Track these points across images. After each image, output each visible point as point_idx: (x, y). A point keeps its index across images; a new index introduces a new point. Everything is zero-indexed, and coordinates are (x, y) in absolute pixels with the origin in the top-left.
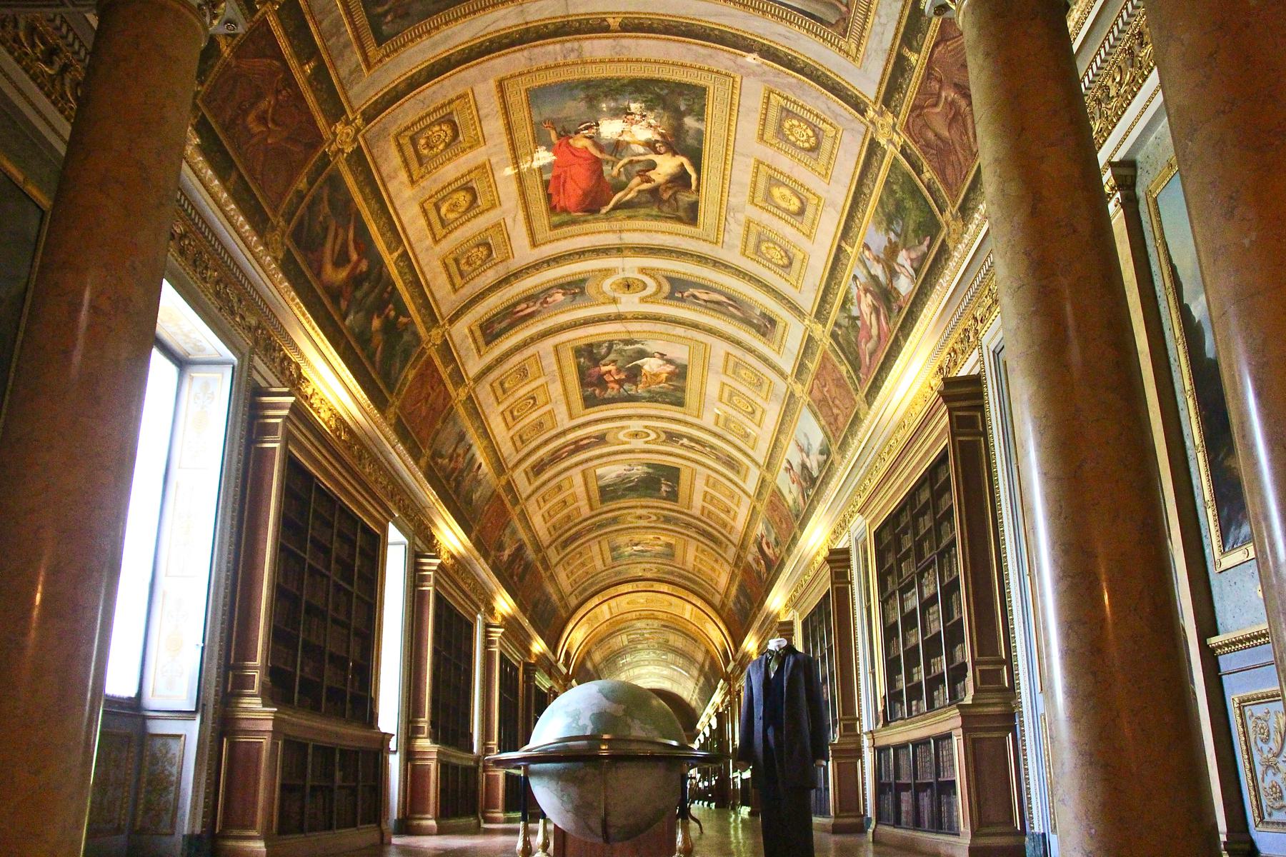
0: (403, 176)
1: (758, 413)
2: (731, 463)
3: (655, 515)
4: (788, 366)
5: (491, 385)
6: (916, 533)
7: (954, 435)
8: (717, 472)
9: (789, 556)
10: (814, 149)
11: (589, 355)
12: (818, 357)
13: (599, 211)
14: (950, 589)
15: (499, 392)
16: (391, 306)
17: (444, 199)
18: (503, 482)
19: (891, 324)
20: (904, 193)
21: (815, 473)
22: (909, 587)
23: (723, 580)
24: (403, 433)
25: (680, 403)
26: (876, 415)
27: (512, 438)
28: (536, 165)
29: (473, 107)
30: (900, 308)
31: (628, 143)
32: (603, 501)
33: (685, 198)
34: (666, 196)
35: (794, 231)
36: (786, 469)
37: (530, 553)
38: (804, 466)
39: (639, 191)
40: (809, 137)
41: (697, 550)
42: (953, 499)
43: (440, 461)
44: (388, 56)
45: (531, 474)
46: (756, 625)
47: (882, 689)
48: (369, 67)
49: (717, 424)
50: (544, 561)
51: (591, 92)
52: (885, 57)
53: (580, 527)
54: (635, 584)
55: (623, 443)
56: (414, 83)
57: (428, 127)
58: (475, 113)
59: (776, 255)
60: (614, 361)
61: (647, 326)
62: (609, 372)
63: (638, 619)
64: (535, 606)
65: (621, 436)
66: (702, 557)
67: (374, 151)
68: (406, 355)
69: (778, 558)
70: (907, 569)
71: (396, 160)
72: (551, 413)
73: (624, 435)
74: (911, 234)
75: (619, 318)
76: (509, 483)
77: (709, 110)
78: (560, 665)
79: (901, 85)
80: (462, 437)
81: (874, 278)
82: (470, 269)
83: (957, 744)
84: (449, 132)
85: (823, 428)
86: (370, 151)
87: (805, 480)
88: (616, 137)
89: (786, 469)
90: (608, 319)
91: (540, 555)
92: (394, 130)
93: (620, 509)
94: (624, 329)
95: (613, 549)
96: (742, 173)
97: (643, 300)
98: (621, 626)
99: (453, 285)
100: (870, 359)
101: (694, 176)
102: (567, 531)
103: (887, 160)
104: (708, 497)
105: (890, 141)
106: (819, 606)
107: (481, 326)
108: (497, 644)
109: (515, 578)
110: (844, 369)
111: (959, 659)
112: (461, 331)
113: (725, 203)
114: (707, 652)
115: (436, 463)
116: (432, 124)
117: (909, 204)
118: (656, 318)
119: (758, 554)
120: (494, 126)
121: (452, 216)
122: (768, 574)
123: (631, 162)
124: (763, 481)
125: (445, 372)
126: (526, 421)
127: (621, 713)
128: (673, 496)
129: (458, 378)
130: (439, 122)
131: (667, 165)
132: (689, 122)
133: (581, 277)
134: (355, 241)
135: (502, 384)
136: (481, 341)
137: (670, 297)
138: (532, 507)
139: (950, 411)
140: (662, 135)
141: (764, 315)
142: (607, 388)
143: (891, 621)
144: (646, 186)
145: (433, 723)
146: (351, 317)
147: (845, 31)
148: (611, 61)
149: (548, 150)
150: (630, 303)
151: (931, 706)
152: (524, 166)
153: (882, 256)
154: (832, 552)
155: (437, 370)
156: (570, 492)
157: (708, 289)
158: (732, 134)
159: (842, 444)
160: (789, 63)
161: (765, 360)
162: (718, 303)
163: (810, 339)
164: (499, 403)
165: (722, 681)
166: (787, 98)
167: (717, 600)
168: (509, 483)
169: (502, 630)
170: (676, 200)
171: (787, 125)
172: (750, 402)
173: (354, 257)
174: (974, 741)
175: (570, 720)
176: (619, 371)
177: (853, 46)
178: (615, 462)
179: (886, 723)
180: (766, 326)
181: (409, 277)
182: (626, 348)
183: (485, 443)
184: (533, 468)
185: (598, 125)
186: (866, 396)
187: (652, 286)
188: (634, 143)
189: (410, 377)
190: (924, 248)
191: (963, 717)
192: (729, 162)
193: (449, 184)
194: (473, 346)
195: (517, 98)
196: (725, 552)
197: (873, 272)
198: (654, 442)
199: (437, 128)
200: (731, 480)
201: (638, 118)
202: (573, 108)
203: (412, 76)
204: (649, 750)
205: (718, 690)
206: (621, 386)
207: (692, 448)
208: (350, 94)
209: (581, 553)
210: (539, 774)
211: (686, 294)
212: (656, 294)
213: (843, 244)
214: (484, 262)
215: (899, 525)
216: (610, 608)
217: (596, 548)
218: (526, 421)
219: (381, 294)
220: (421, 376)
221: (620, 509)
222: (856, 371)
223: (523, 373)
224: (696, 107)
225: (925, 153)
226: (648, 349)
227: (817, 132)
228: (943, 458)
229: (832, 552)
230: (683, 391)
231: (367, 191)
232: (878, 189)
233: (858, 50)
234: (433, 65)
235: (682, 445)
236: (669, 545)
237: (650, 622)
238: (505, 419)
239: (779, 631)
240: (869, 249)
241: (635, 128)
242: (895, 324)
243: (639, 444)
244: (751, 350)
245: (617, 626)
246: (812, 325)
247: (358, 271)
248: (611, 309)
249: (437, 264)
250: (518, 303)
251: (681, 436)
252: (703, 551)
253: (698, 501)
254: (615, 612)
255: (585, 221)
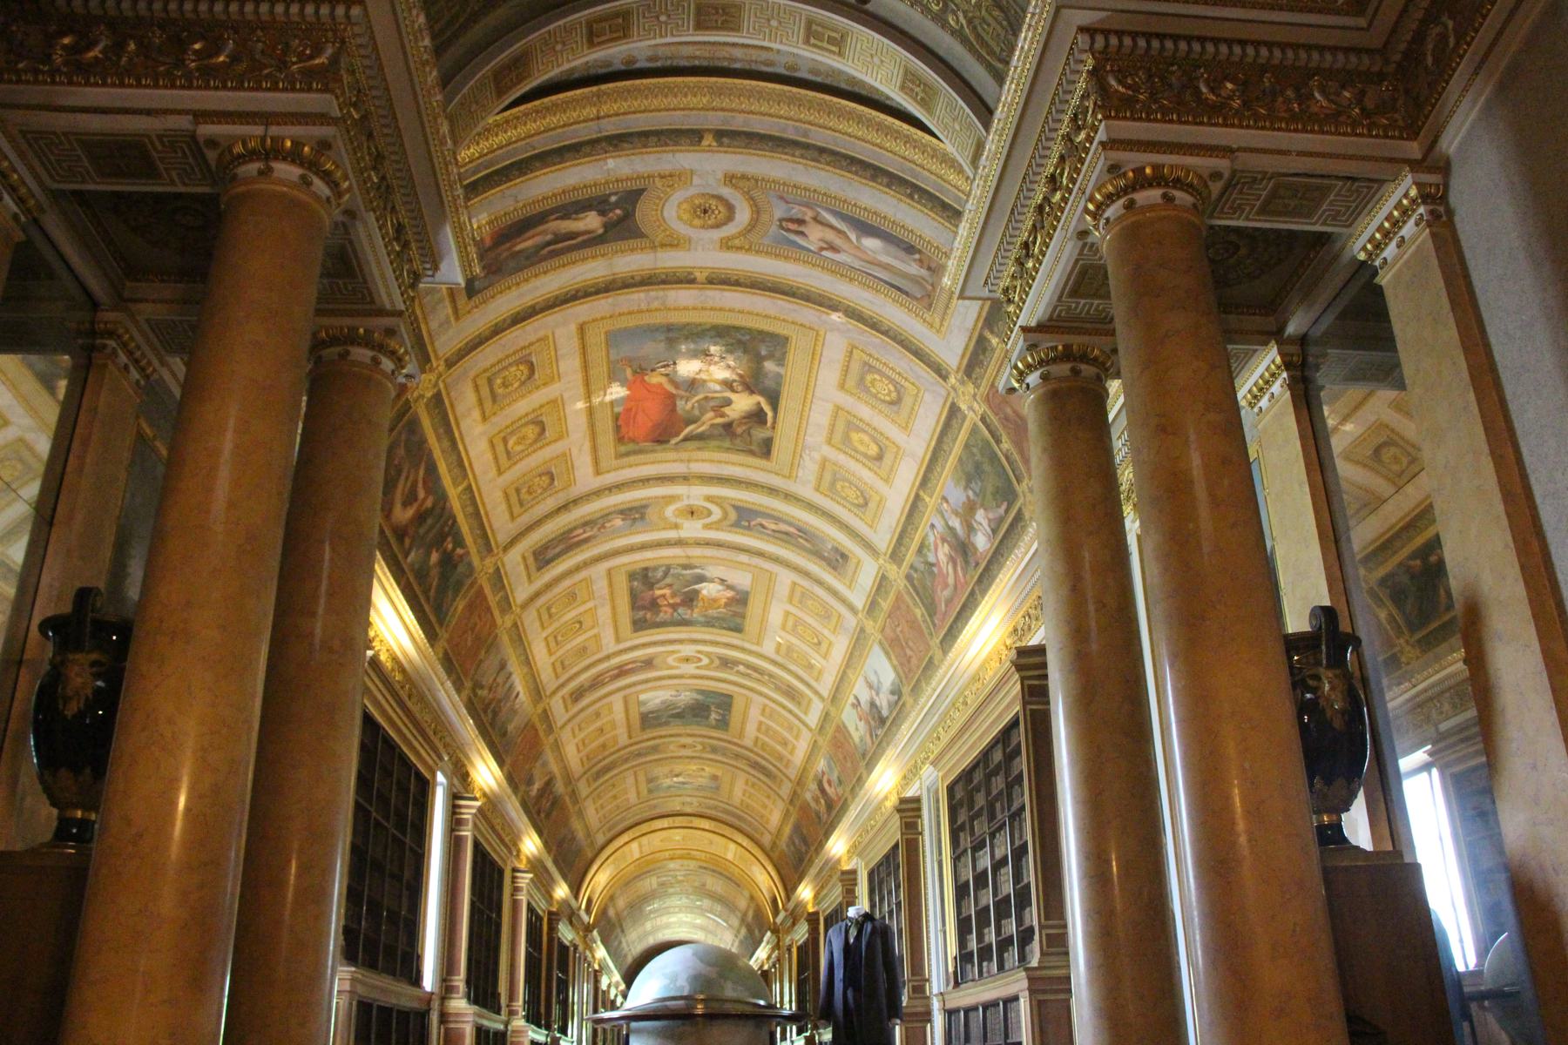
0: (476, 414)
1: (824, 646)
2: (791, 693)
3: (702, 744)
4: (859, 601)
5: (538, 611)
6: (988, 793)
7: (1025, 704)
8: (774, 701)
9: (854, 798)
10: (892, 403)
11: (644, 578)
12: (892, 596)
13: (667, 442)
14: (1020, 853)
15: (545, 617)
16: (449, 539)
17: (512, 433)
18: (540, 711)
19: (968, 577)
20: (982, 455)
21: (885, 713)
22: (981, 845)
23: (775, 818)
24: (448, 663)
25: (738, 629)
26: (951, 665)
27: (553, 664)
28: (608, 398)
29: (552, 348)
30: (977, 564)
31: (705, 381)
32: (643, 728)
33: (760, 434)
34: (739, 430)
35: (870, 474)
36: (853, 705)
37: (560, 787)
38: (873, 704)
39: (712, 425)
40: (890, 391)
41: (747, 784)
42: (1023, 764)
43: (480, 692)
44: (477, 307)
45: (569, 702)
46: (813, 871)
47: (953, 949)
48: (457, 318)
49: (778, 652)
50: (574, 794)
51: (671, 335)
52: (968, 334)
53: (614, 757)
54: (670, 819)
55: (672, 668)
56: (497, 330)
57: (505, 368)
58: (553, 353)
59: (852, 494)
60: (670, 586)
61: (709, 552)
62: (664, 596)
63: (672, 859)
64: (560, 845)
65: (670, 660)
66: (752, 791)
67: (452, 394)
68: (459, 584)
69: (840, 799)
70: (981, 827)
71: (471, 397)
72: (597, 637)
73: (674, 660)
74: (989, 496)
75: (680, 543)
76: (545, 711)
77: (790, 357)
78: (583, 913)
79: (982, 362)
80: (503, 666)
81: (951, 529)
82: (529, 498)
83: (1024, 1005)
84: (526, 372)
85: (895, 668)
86: (448, 394)
87: (873, 718)
88: (692, 375)
89: (853, 705)
90: (668, 544)
91: (570, 789)
92: (472, 374)
93: (661, 737)
94: (683, 554)
95: (650, 781)
96: (820, 416)
97: (707, 527)
98: (651, 867)
99: (511, 514)
100: (946, 606)
101: (770, 415)
102: (600, 761)
103: (967, 425)
104: (763, 728)
105: (971, 408)
106: (887, 857)
107: (534, 553)
108: (525, 892)
109: (543, 815)
110: (919, 612)
111: (1027, 923)
112: (513, 561)
113: (801, 441)
114: (752, 898)
115: (476, 695)
116: (510, 365)
117: (987, 467)
118: (719, 545)
119: (818, 793)
120: (570, 364)
121: (519, 448)
122: (829, 815)
123: (706, 398)
124: (827, 714)
125: (493, 600)
126: (568, 646)
127: (714, 976)
128: (723, 724)
129: (506, 605)
130: (517, 363)
131: (743, 403)
132: (769, 366)
133: (644, 502)
134: (425, 482)
135: (549, 609)
136: (533, 566)
137: (737, 525)
138: (566, 735)
139: (1023, 679)
140: (741, 376)
141: (836, 550)
142: (657, 613)
143: (963, 879)
144: (719, 420)
145: (468, 982)
146: (413, 554)
147: (930, 305)
148: (695, 309)
149: (622, 386)
150: (692, 529)
151: (1001, 967)
152: (596, 400)
153: (960, 510)
154: (903, 801)
155: (485, 598)
156: (609, 718)
157: (778, 519)
158: (813, 380)
159: (915, 686)
160: (874, 325)
161: (834, 593)
162: (787, 533)
163: (884, 577)
164: (543, 627)
165: (769, 934)
166: (870, 355)
167: (766, 840)
168: (545, 711)
169: (531, 875)
170: (749, 434)
171: (869, 378)
172: (816, 633)
173: (421, 494)
174: (1040, 1002)
175: (667, 982)
176: (674, 595)
177: (937, 320)
178: (660, 687)
179: (957, 984)
180: (838, 560)
181: (470, 509)
182: (684, 572)
183: (525, 670)
184: (572, 694)
185: (675, 363)
186: (941, 642)
187: (717, 514)
188: (711, 381)
189: (460, 607)
190: (1002, 510)
191: (1030, 979)
192: (808, 405)
193: (520, 419)
194: (524, 574)
195: (596, 338)
196: (779, 787)
197: (950, 523)
198: (706, 667)
199: (514, 369)
200: (790, 712)
201: (716, 359)
202: (652, 348)
203: (496, 324)
204: (740, 1008)
205: (763, 944)
206: (675, 610)
207: (748, 675)
208: (437, 344)
209: (614, 786)
210: (639, 1031)
211: (753, 523)
212: (720, 521)
213: (921, 493)
214: (545, 490)
215: (971, 781)
216: (640, 846)
217: (631, 780)
218: (568, 646)
219: (442, 527)
220: (471, 607)
221: (661, 737)
222: (930, 616)
223: (572, 597)
224: (778, 354)
225: (1005, 427)
226: (708, 574)
227: (899, 390)
228: (1014, 724)
229: (903, 801)
230: (743, 617)
231: (441, 431)
232: (957, 449)
233: (941, 325)
234: (518, 313)
235: (738, 672)
236: (715, 778)
237: (686, 862)
238: (548, 645)
239: (841, 881)
240: (947, 502)
241: (712, 368)
242: (972, 577)
243: (690, 669)
244: (820, 582)
245: (647, 867)
246: (887, 565)
247: (424, 508)
248: (672, 534)
249: (499, 494)
250: (575, 528)
251: (736, 662)
252: (753, 785)
253: (751, 730)
254: (646, 850)
255: (652, 451)
